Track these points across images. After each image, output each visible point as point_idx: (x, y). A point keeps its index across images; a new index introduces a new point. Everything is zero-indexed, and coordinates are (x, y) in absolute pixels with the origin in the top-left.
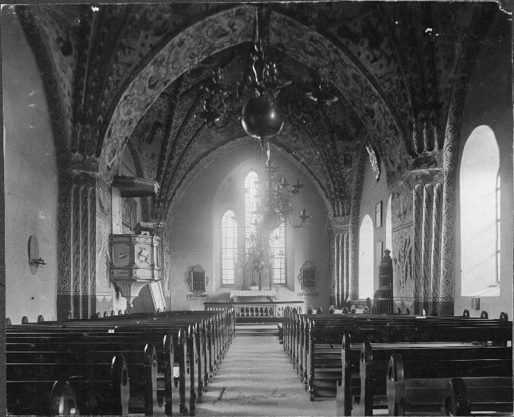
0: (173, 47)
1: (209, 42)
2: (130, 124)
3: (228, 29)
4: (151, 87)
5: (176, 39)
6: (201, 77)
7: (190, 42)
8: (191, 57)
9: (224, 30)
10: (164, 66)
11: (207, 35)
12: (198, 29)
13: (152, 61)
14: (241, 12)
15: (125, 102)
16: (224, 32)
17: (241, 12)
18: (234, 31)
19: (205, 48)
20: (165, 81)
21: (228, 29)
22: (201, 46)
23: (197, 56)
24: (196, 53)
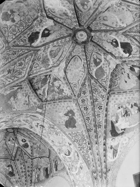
0: (54, 145)
1: (48, 130)
2: (81, 168)
3: (39, 127)
4: (69, 155)
5: (51, 144)
6: (129, 42)
7: (52, 138)
8: (57, 135)
9: (40, 128)
10: (61, 148)
11: (46, 132)
12: (46, 137)
13: (59, 155)
14: (31, 127)
15: (70, 169)
16: (42, 127)
17: (31, 127)
18: (38, 124)
19: (52, 129)
20: (68, 145)
21: (39, 127)
22: (51, 132)
23: (56, 131)
24: (55, 132)
